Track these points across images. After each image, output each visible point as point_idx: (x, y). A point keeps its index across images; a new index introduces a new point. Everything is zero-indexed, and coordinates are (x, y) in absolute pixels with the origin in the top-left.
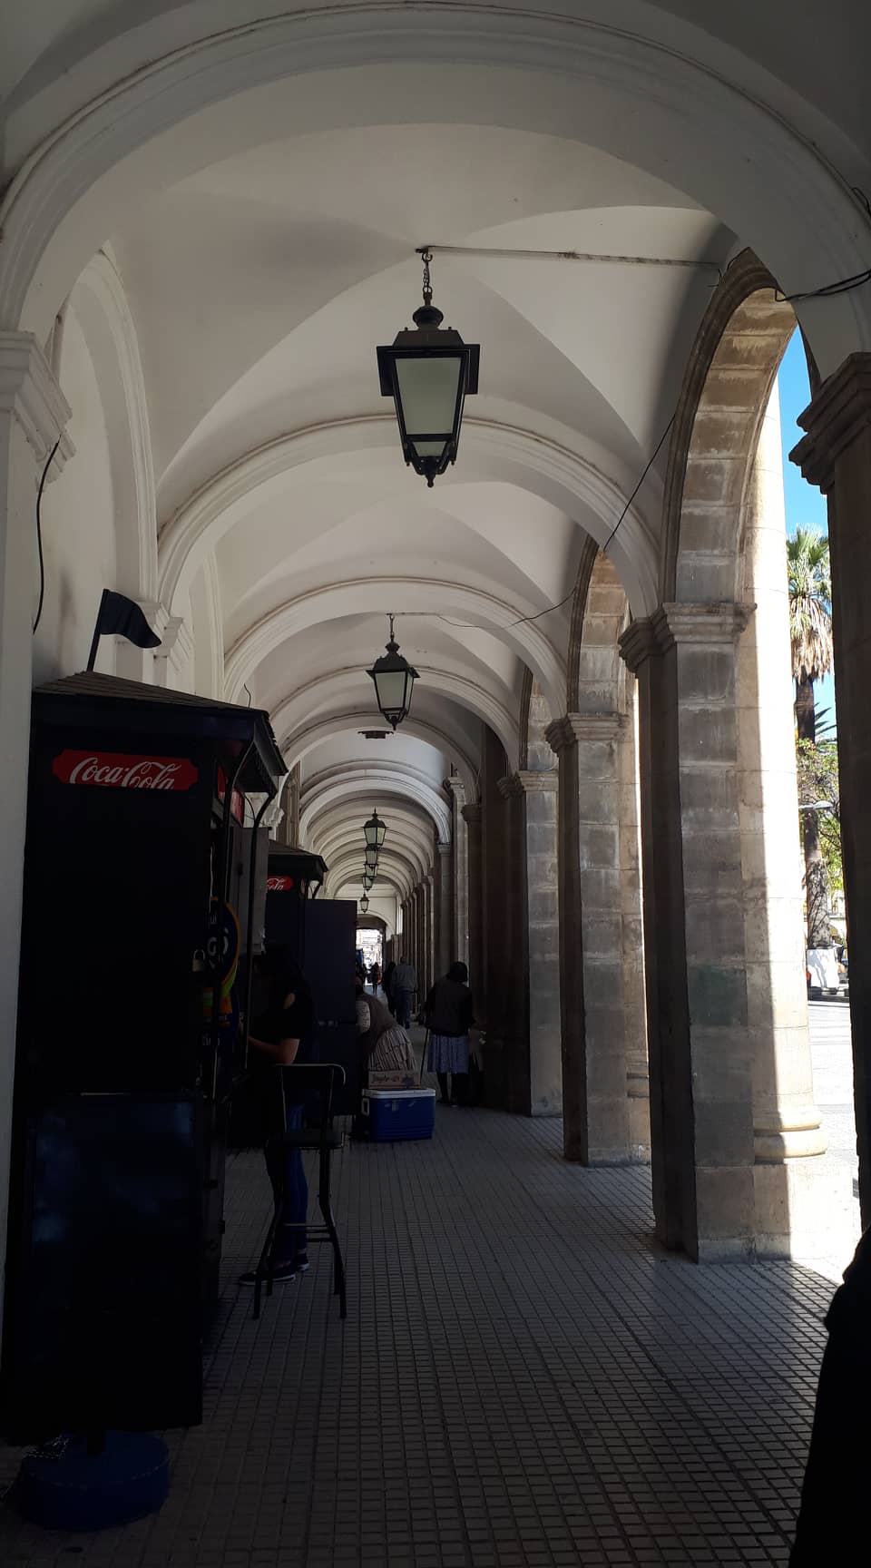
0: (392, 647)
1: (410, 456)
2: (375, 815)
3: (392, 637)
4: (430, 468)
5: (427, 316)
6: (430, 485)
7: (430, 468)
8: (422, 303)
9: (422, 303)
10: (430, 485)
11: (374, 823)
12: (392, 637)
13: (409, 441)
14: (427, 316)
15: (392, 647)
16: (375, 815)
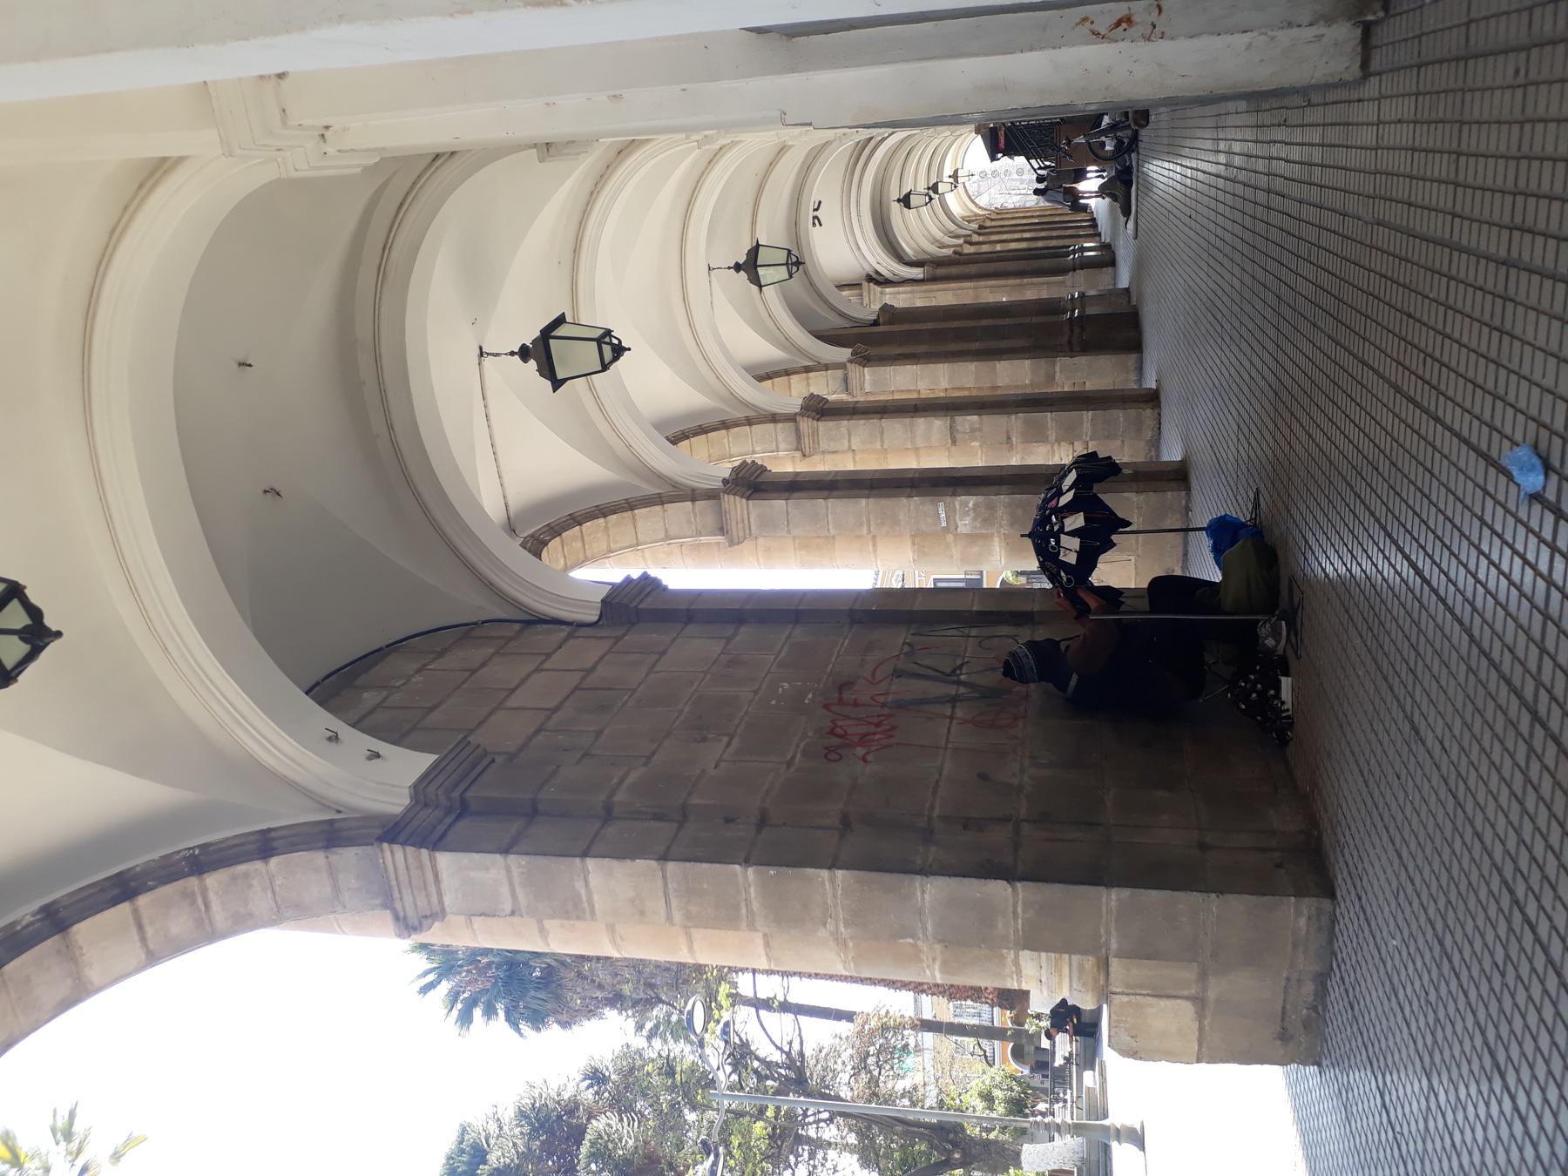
0: (738, 267)
1: (615, 359)
2: (899, 200)
3: (729, 268)
4: (619, 351)
5: (524, 353)
6: (629, 349)
7: (619, 351)
8: (517, 357)
9: (517, 357)
10: (629, 349)
11: (906, 201)
12: (729, 268)
13: (605, 367)
14: (524, 353)
15: (738, 267)
16: (899, 200)
